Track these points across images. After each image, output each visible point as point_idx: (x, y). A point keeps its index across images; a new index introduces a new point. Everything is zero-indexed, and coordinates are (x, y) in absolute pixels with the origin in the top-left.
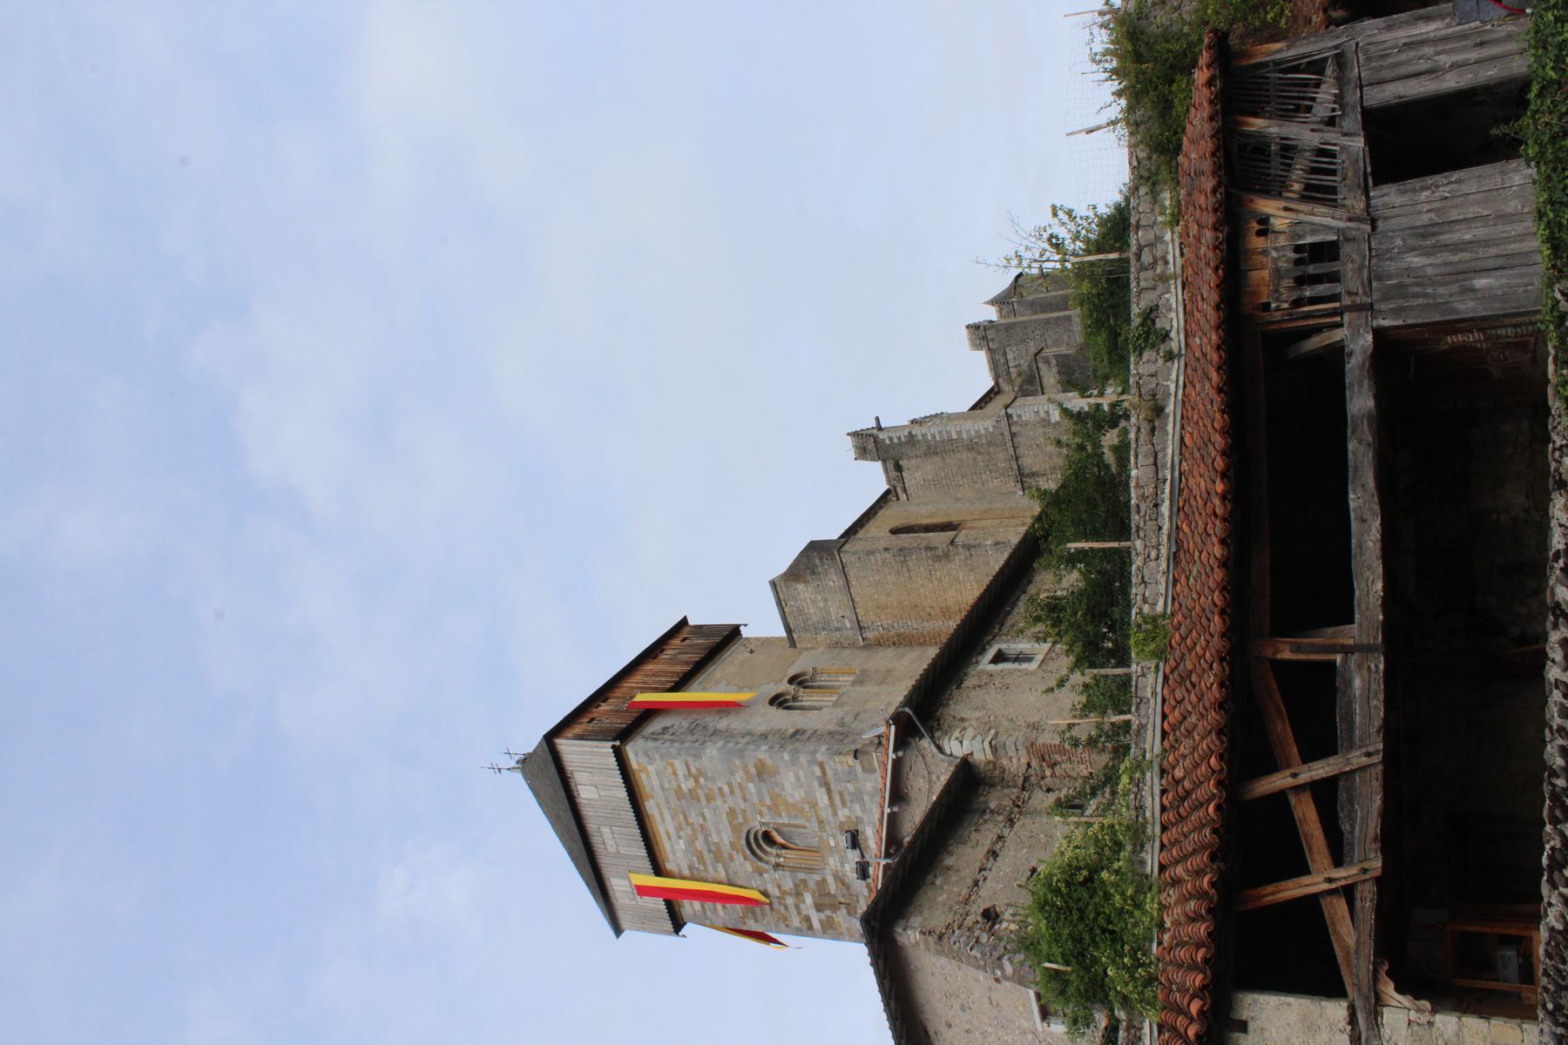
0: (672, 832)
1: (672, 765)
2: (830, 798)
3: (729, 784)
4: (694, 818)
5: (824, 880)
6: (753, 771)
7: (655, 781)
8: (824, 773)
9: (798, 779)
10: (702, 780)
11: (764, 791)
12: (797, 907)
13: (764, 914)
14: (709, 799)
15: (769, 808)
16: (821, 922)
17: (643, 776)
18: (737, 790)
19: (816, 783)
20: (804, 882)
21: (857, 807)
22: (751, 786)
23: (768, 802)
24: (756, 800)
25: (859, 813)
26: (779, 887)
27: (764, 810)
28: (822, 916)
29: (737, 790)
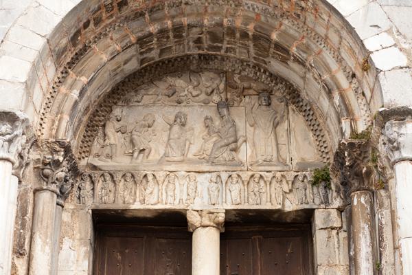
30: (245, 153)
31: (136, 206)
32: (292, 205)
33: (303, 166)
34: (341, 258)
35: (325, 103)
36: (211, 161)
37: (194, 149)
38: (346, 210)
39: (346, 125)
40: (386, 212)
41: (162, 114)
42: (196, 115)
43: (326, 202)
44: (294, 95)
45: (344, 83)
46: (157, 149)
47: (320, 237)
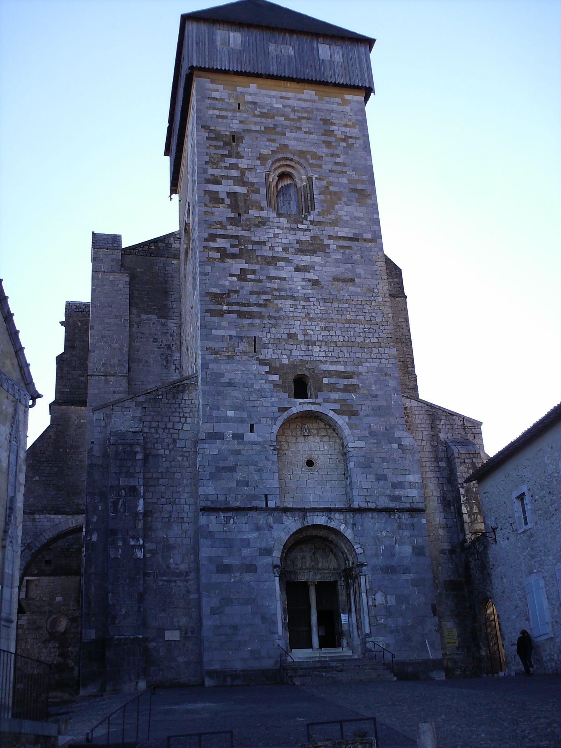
0: (290, 102)
1: (353, 126)
2: (344, 238)
3: (343, 164)
4: (306, 125)
5: (262, 209)
6: (360, 187)
7: (335, 107)
8: (365, 240)
9: (358, 218)
10: (344, 144)
11: (342, 189)
12: (229, 178)
13: (217, 147)
14: (328, 144)
15: (327, 187)
16: (217, 192)
17: (340, 100)
18: (339, 168)
19: (357, 231)
20: (258, 191)
21: (340, 256)
22: (345, 180)
23: (331, 188)
24: (331, 179)
25: (334, 256)
26: (249, 169)
27: (324, 183)
28: (223, 195)
29: (339, 168)
30: (320, 565)
31: (296, 581)
32: (332, 579)
33: (335, 569)
34: (344, 592)
35: (341, 555)
36: (313, 568)
37: (308, 565)
38: (346, 581)
39: (347, 563)
40: (357, 584)
41: (299, 556)
42: (308, 555)
43: (340, 579)
44: (332, 550)
45: (346, 551)
46: (299, 566)
47: (339, 587)
